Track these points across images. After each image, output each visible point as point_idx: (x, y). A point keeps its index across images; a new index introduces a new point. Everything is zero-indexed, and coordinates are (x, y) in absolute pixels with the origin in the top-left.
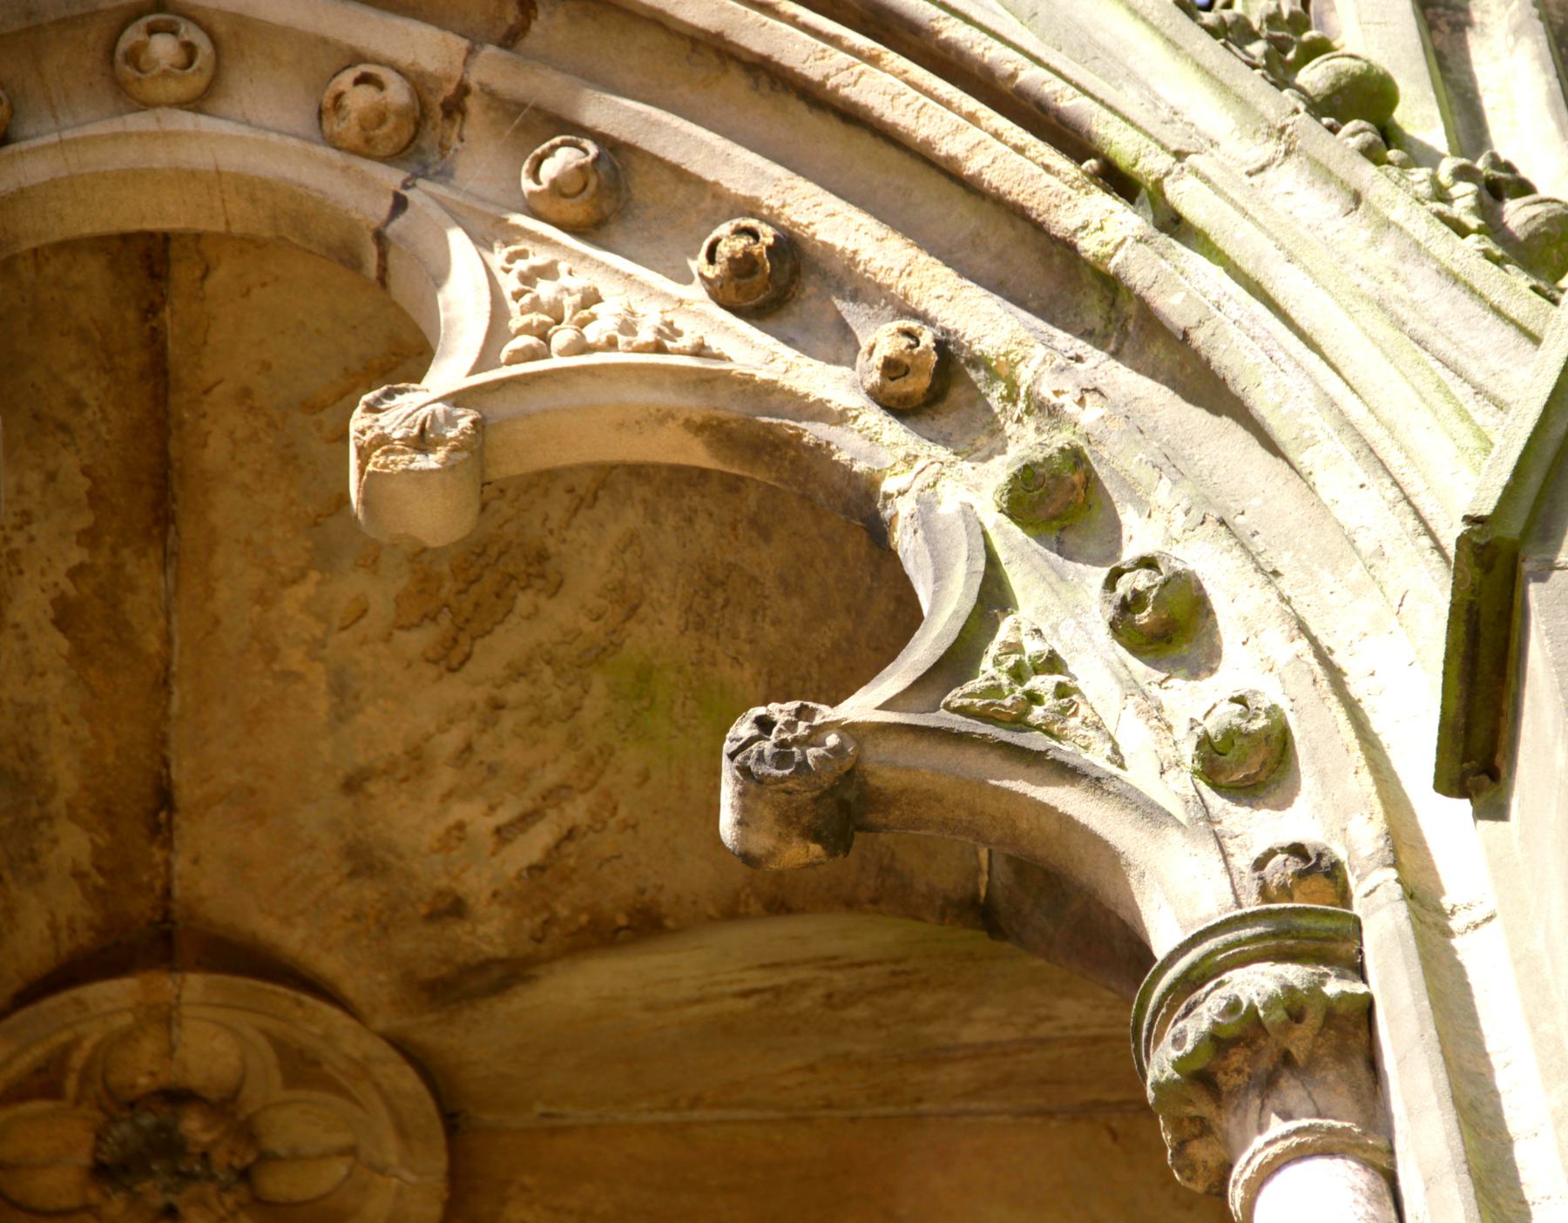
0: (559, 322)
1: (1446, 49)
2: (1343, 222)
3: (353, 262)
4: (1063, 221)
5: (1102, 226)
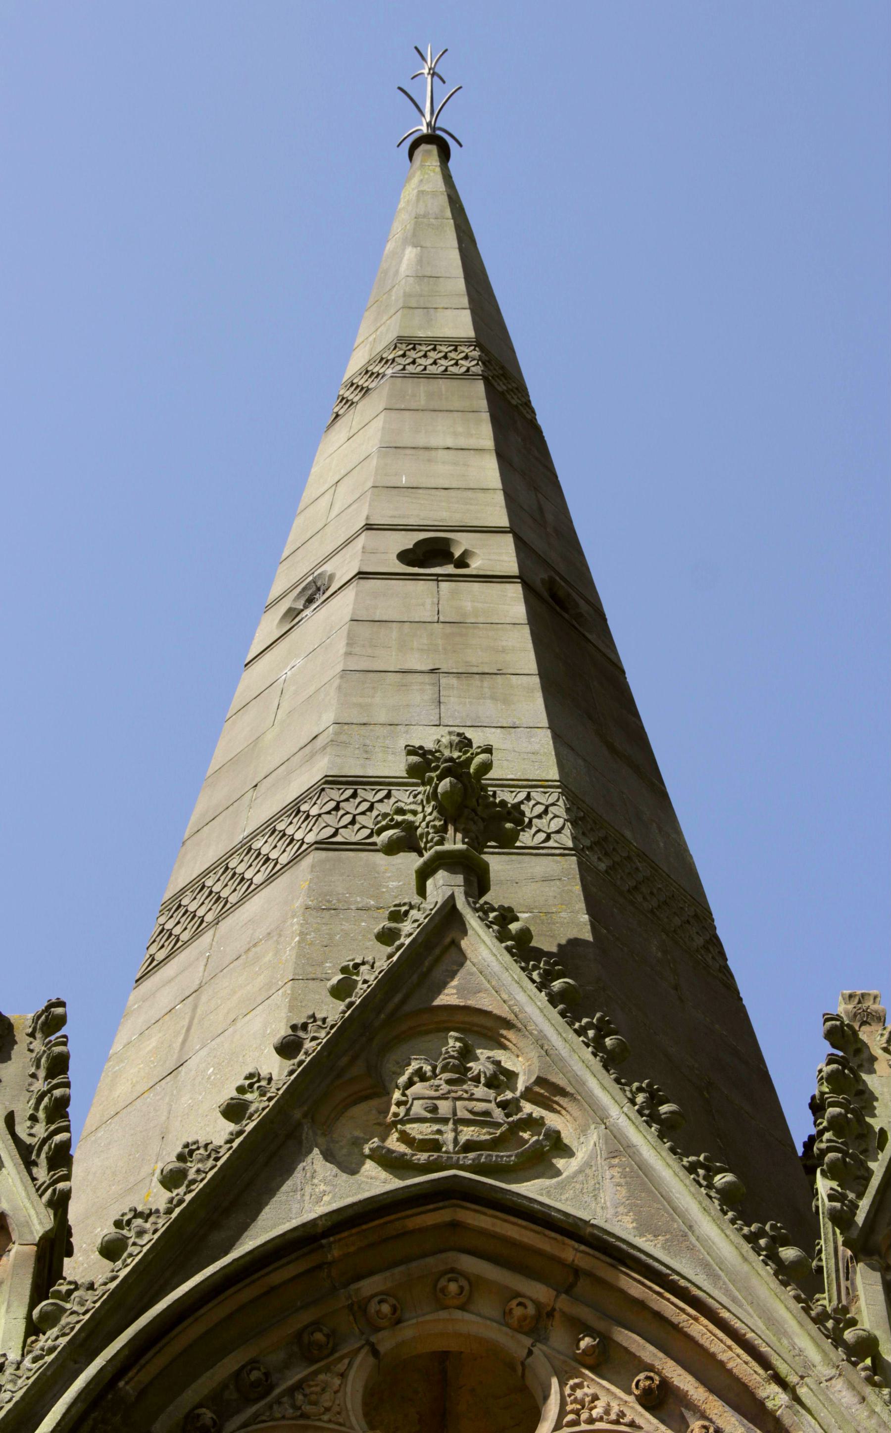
0: (583, 1408)
2: (858, 1406)
3: (514, 1370)
4: (762, 1393)
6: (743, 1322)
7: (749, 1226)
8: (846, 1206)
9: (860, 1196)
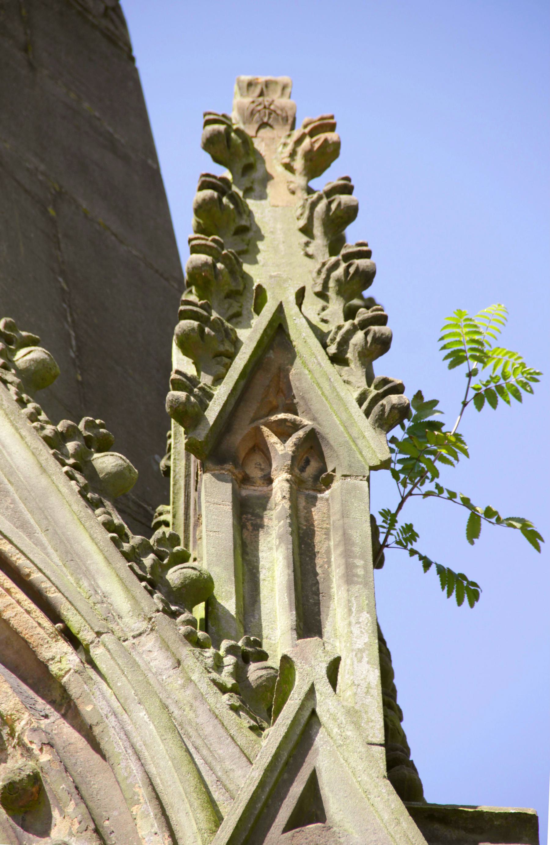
1: (248, 541)
2: (172, 672)
4: (45, 654)
5: (62, 659)
6: (28, 558)
7: (55, 423)
8: (195, 396)
9: (218, 380)
